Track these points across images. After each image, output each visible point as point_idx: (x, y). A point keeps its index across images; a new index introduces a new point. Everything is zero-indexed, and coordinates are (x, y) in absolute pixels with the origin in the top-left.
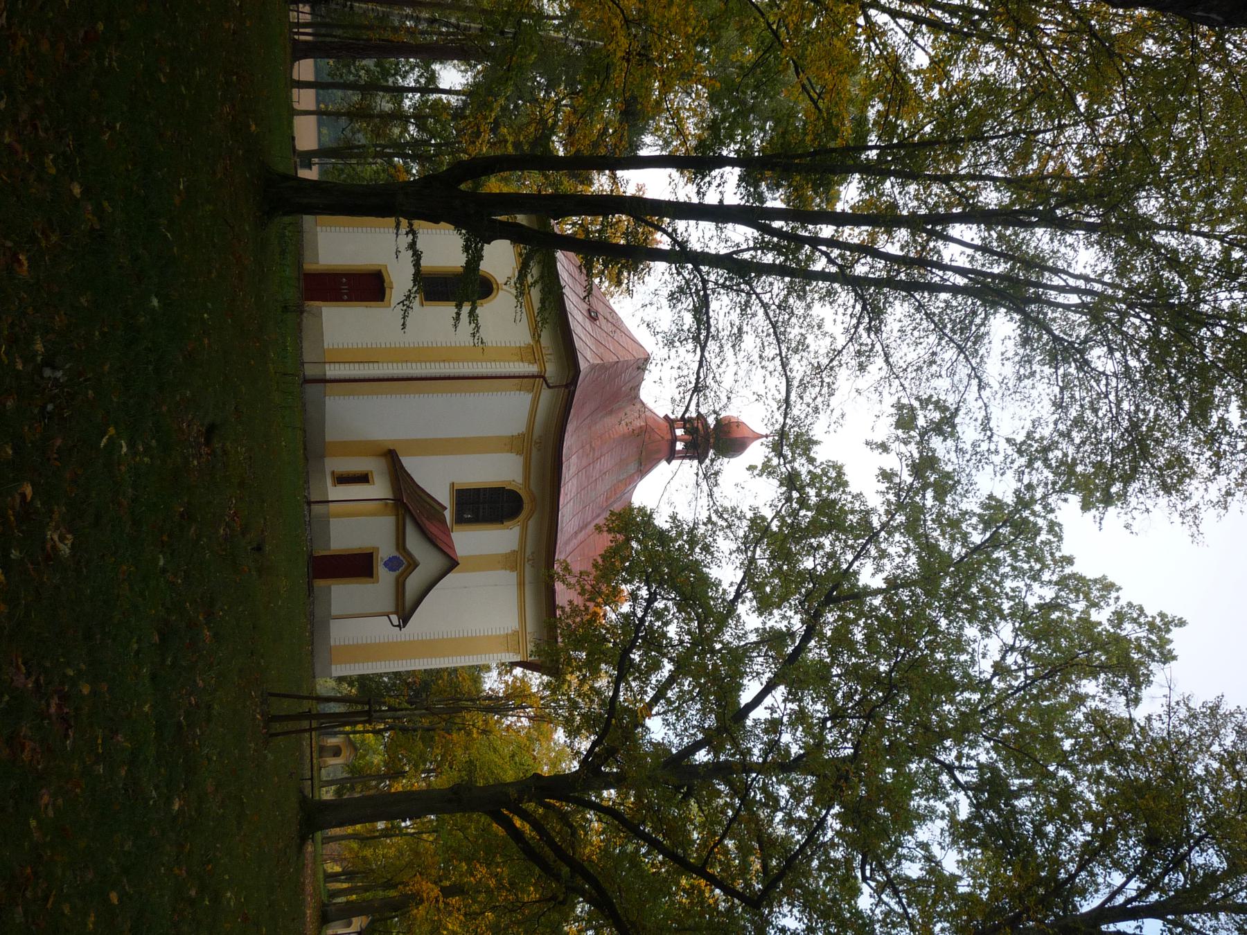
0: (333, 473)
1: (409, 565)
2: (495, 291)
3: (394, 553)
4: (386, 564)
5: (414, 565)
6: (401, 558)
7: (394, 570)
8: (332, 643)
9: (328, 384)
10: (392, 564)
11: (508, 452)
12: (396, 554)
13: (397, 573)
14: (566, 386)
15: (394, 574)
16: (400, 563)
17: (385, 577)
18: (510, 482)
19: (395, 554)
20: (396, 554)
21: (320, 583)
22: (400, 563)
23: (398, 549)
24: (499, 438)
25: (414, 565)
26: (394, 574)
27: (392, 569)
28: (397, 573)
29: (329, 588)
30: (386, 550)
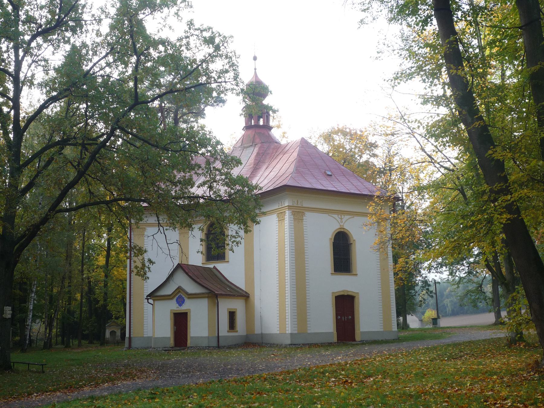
3: (174, 301)
4: (180, 305)
5: (179, 289)
6: (177, 297)
7: (184, 300)
8: (278, 332)
9: (132, 336)
10: (180, 302)
12: (175, 299)
13: (185, 299)
15: (187, 300)
17: (188, 305)
19: (174, 301)
20: (175, 299)
21: (189, 343)
22: (180, 297)
23: (172, 299)
25: (179, 289)
26: (187, 300)
27: (183, 302)
29: (192, 338)
30: (173, 306)
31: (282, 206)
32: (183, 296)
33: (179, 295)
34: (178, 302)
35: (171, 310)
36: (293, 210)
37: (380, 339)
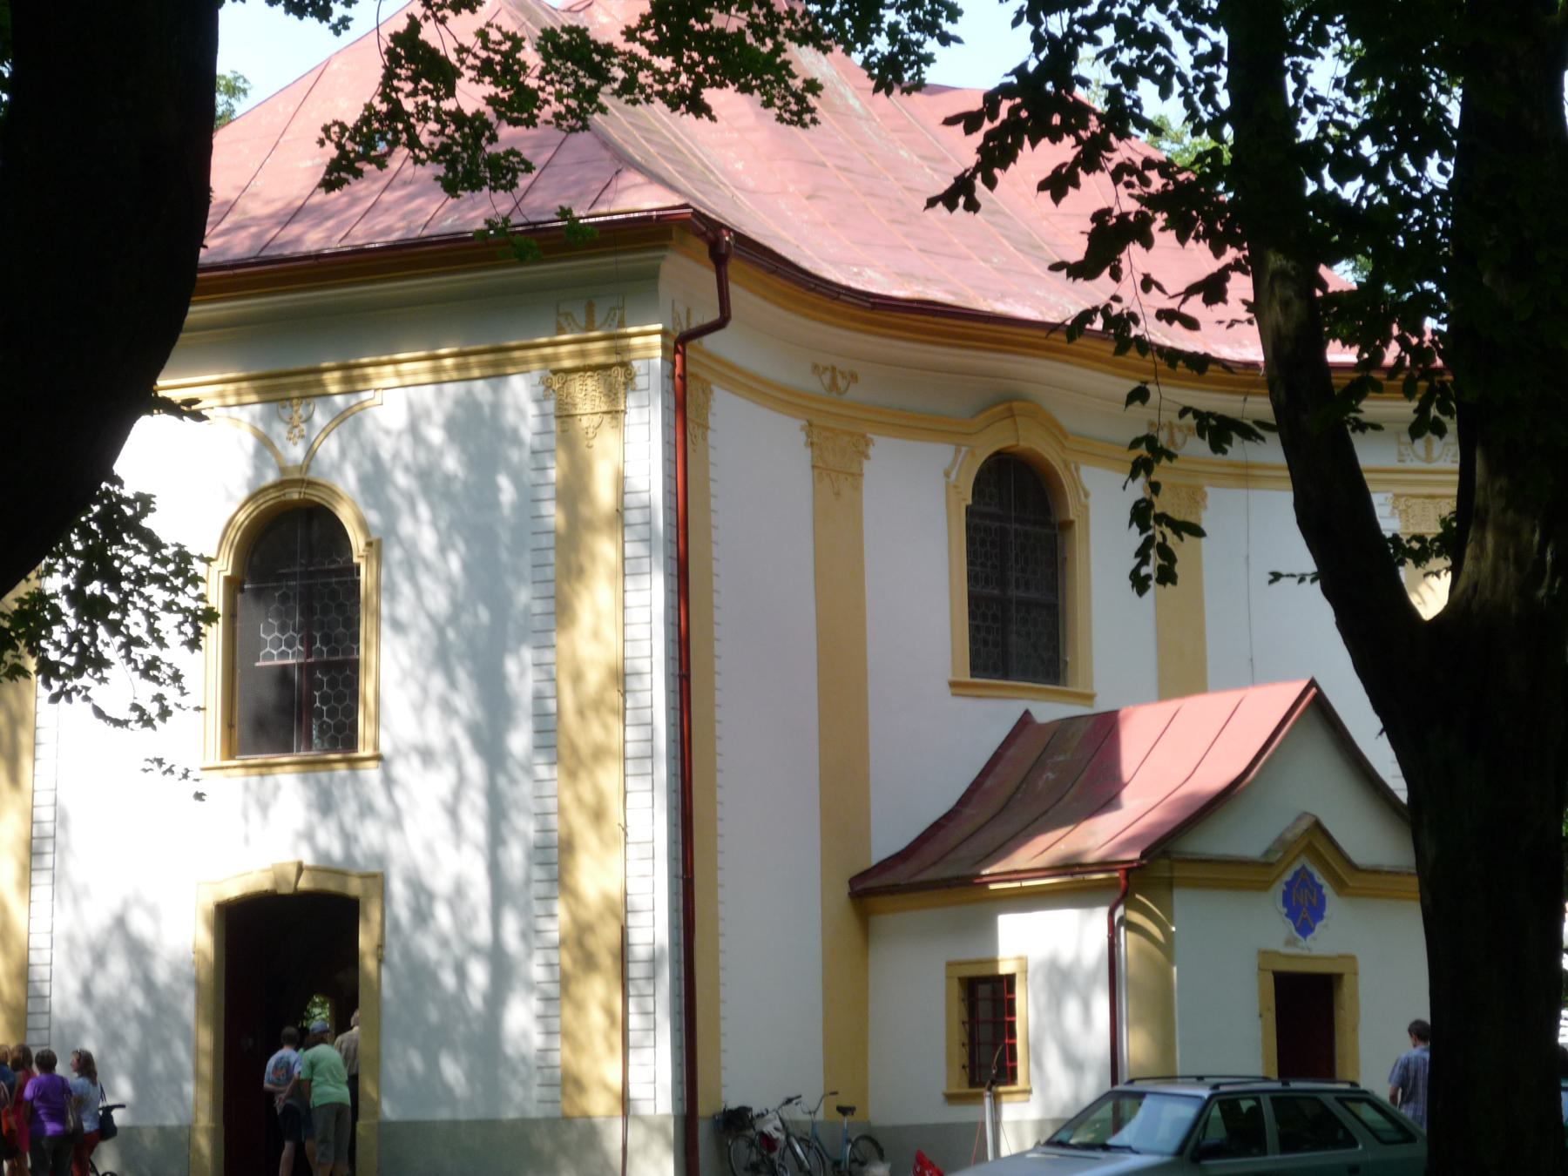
0: (951, 1098)
1: (1311, 850)
2: (316, 496)
4: (1305, 929)
6: (1288, 877)
7: (1322, 900)
11: (857, 488)
12: (1278, 889)
13: (1328, 891)
14: (719, 258)
16: (1303, 878)
18: (951, 488)
22: (1303, 878)
23: (1264, 886)
24: (820, 517)
26: (1335, 906)
27: (1317, 911)
28: (1328, 891)
31: (1429, 459)
32: (1320, 879)
33: (1296, 866)
34: (1293, 913)
35: (1264, 954)
36: (1399, 490)
37: (1174, 1098)
